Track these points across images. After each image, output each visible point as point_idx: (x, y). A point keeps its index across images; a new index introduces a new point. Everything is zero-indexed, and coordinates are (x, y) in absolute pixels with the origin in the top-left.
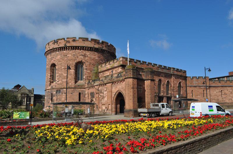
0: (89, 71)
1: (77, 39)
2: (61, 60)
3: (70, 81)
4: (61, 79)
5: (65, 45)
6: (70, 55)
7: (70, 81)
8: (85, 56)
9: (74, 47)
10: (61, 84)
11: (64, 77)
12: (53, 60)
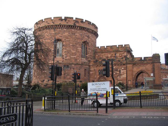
0: (91, 51)
1: (84, 21)
2: (69, 37)
3: (78, 58)
4: (69, 55)
5: (74, 24)
7: (78, 58)
8: (88, 37)
9: (82, 27)
10: (68, 59)
11: (73, 54)
12: (57, 36)
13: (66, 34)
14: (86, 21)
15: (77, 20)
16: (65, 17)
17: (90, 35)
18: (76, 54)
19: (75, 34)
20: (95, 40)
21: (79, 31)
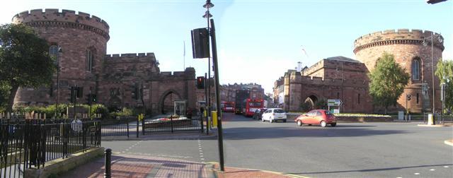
1: (91, 17)
4: (67, 66)
5: (77, 21)
6: (81, 36)
10: (67, 72)
13: (65, 35)
14: (93, 16)
15: (81, 15)
16: (63, 10)
17: (99, 38)
18: (78, 65)
19: (77, 35)
20: (106, 44)
21: (82, 32)
